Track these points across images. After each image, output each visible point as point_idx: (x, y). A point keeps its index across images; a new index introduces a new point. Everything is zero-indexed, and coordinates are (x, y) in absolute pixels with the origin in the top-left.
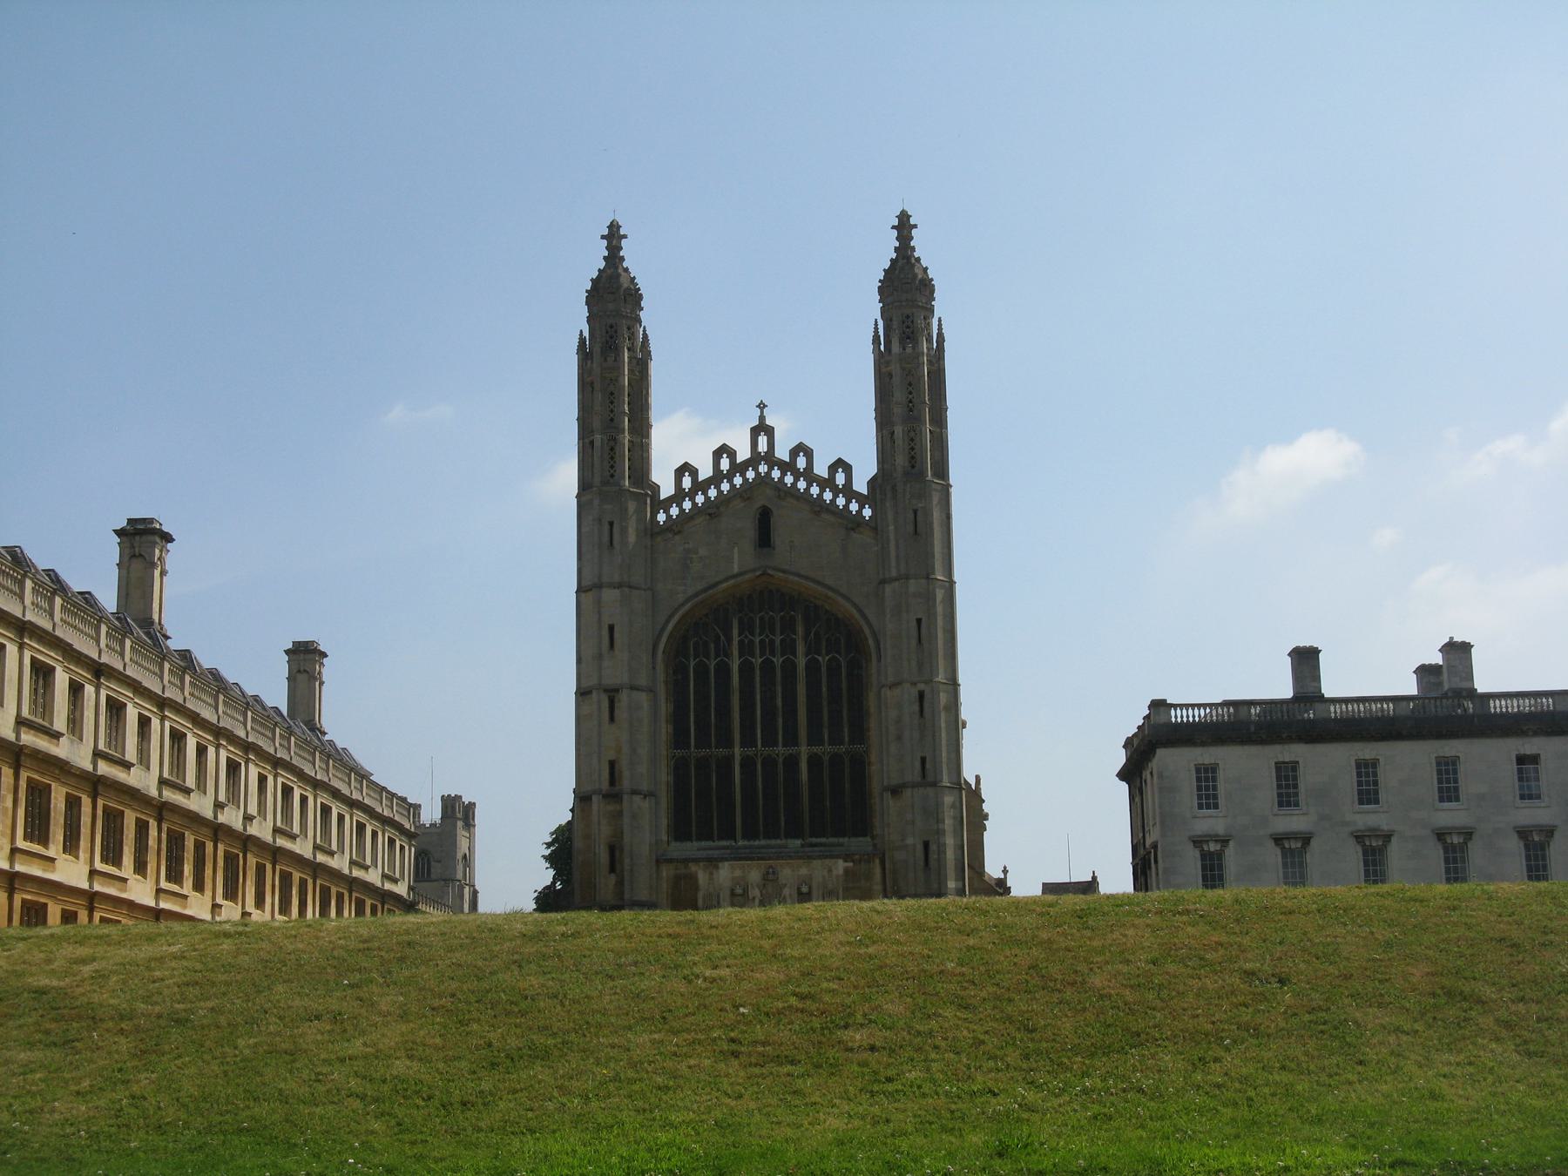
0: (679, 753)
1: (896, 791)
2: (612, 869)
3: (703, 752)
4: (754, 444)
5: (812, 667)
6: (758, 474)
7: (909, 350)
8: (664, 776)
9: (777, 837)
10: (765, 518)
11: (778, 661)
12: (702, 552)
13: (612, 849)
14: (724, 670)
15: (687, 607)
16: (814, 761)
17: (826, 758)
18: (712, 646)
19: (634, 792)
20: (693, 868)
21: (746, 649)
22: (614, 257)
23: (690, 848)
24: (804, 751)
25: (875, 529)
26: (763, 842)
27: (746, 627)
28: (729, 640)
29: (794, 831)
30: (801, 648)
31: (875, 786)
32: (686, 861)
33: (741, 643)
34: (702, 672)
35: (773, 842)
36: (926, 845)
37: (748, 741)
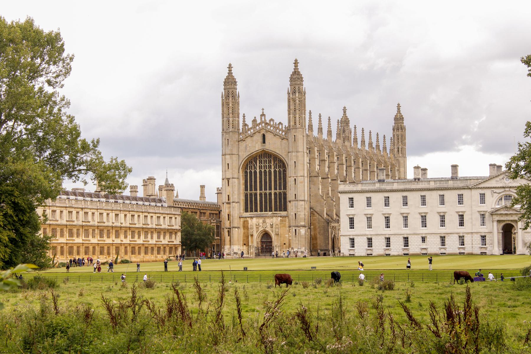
0: (246, 192)
1: (290, 202)
2: (229, 220)
3: (251, 192)
4: (261, 119)
5: (275, 172)
6: (262, 126)
7: (294, 96)
8: (242, 198)
9: (267, 211)
10: (264, 136)
11: (267, 170)
12: (250, 145)
13: (228, 215)
14: (255, 173)
15: (247, 158)
16: (275, 194)
17: (278, 193)
18: (253, 167)
19: (233, 202)
20: (248, 219)
21: (260, 167)
22: (230, 73)
23: (248, 214)
24: (273, 191)
25: (287, 139)
26: (264, 213)
27: (261, 162)
28: (257, 165)
29: (271, 210)
30: (273, 167)
31: (288, 200)
32: (246, 217)
33: (259, 166)
34: (251, 172)
35: (266, 213)
36: (295, 214)
37: (261, 189)
